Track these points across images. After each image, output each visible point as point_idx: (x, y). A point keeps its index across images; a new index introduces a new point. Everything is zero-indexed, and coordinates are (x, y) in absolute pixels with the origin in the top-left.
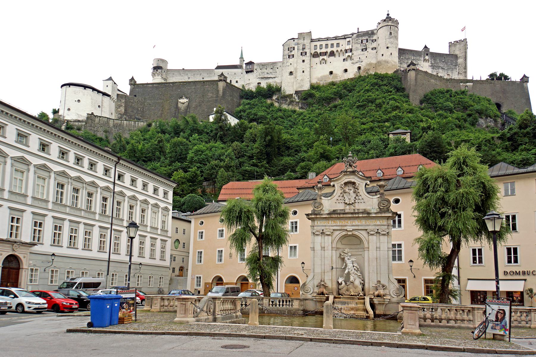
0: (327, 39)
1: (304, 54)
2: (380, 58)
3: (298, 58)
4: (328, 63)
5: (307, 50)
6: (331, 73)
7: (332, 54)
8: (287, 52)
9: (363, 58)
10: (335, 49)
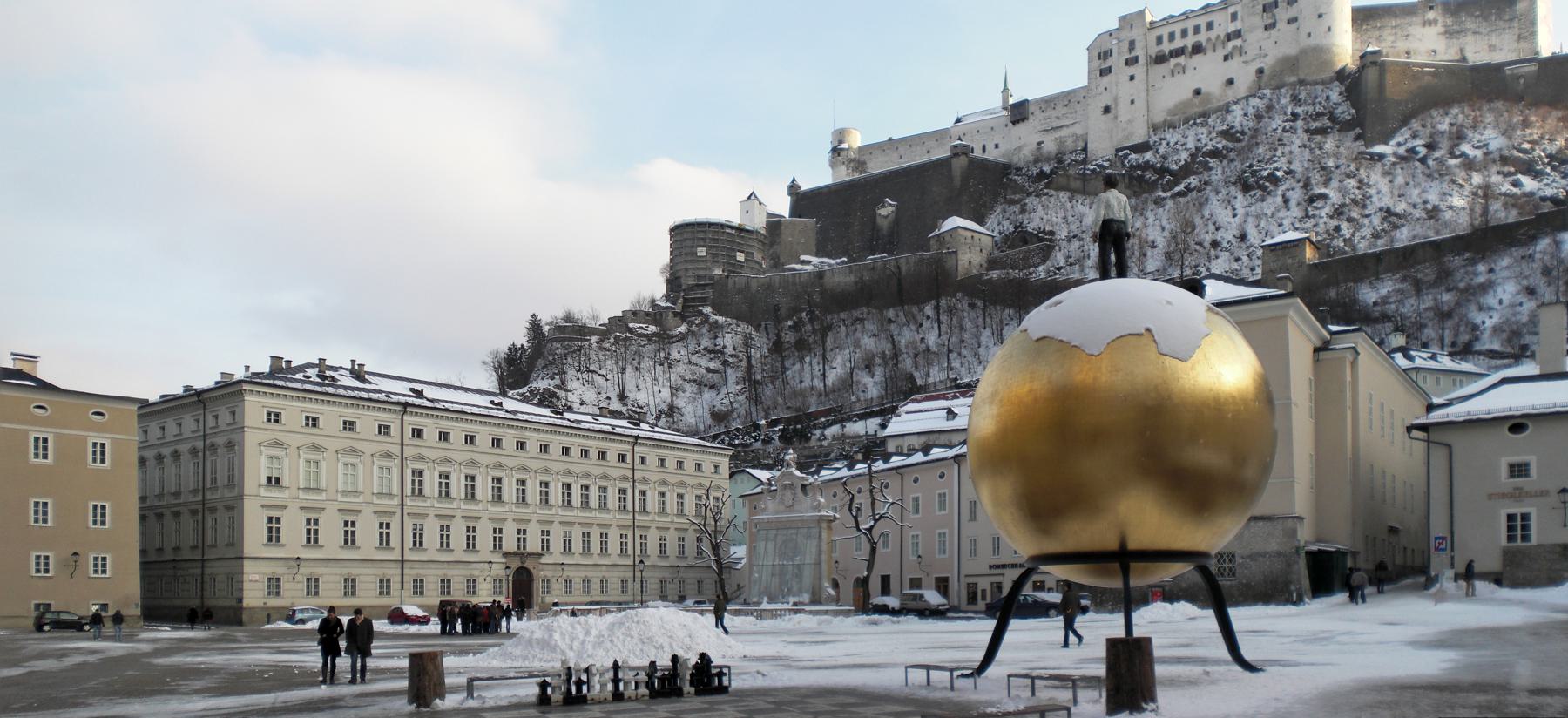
0: (1186, 15)
1: (1132, 61)
2: (1306, 42)
3: (1121, 72)
4: (1189, 72)
5: (1139, 51)
6: (1197, 92)
7: (1198, 49)
8: (1097, 63)
9: (1268, 45)
10: (1202, 37)
